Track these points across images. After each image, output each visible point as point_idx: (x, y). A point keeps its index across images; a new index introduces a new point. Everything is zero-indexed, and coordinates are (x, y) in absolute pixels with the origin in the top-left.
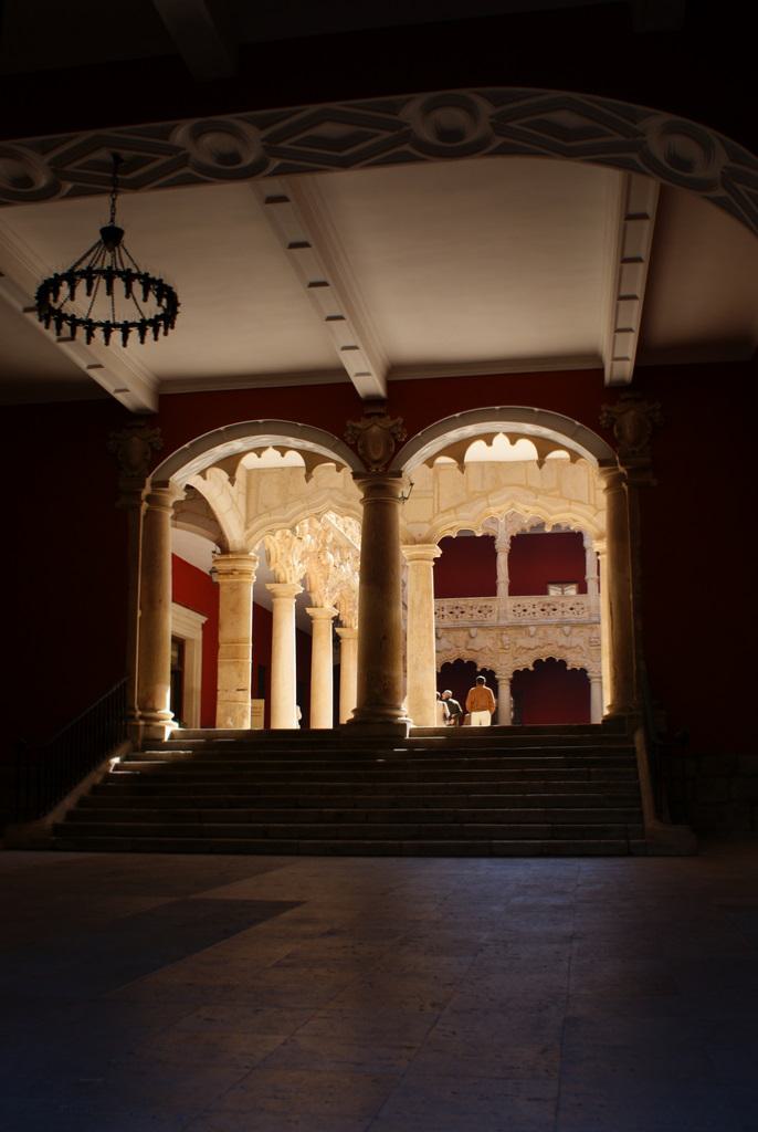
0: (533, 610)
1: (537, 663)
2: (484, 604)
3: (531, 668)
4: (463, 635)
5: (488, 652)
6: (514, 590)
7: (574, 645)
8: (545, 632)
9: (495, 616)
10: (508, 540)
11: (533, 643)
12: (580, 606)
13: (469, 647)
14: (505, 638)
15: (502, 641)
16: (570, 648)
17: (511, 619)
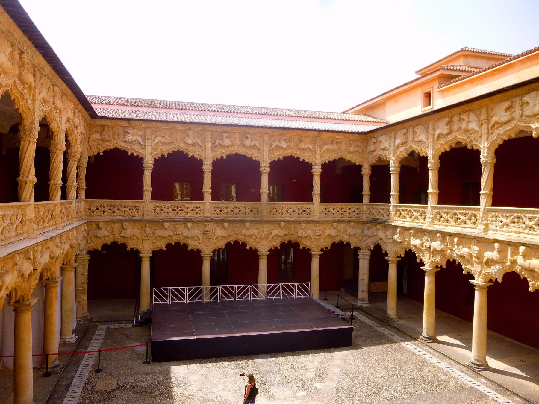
0: (167, 210)
1: (169, 246)
2: (133, 205)
3: (165, 249)
4: (117, 227)
5: (135, 238)
6: (155, 196)
7: (194, 235)
8: (175, 227)
9: (140, 214)
10: (152, 162)
11: (165, 234)
12: (198, 209)
13: (122, 235)
14: (148, 229)
15: (145, 231)
16: (192, 237)
17: (149, 216)
